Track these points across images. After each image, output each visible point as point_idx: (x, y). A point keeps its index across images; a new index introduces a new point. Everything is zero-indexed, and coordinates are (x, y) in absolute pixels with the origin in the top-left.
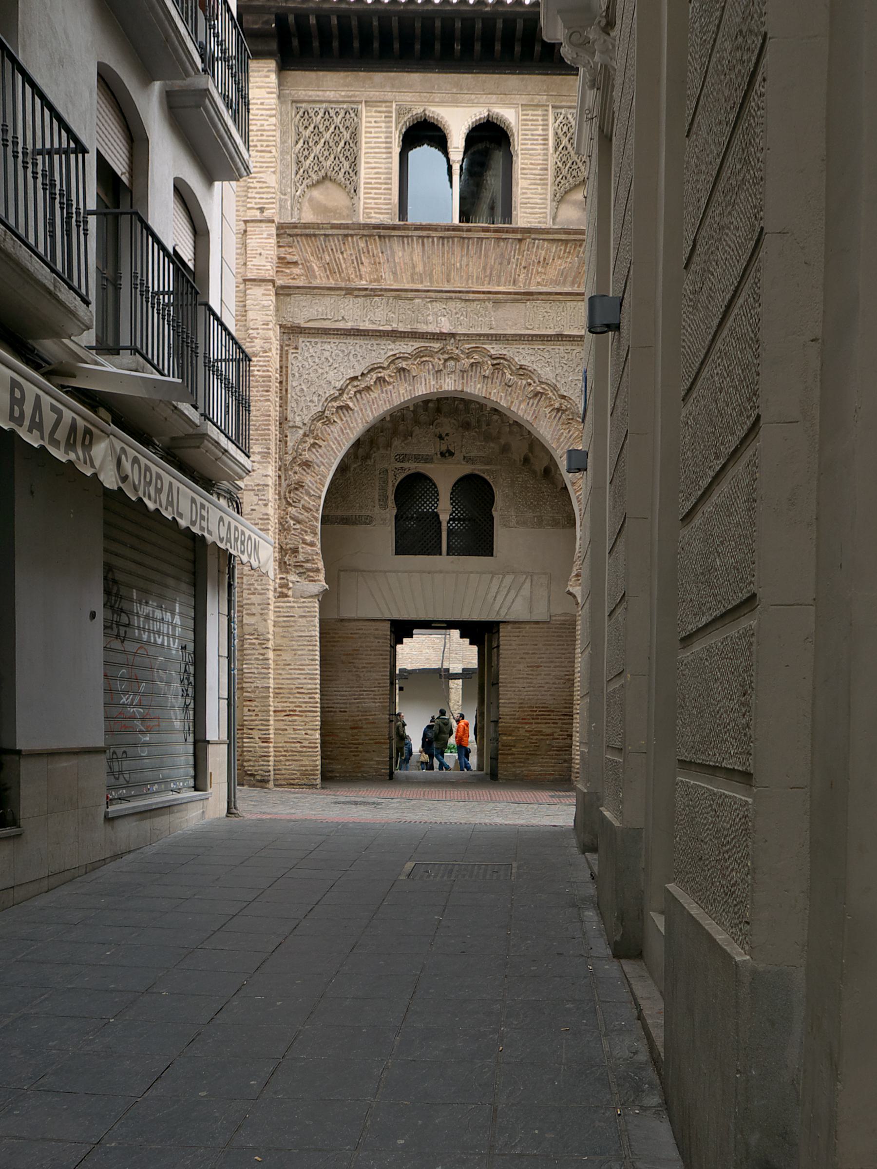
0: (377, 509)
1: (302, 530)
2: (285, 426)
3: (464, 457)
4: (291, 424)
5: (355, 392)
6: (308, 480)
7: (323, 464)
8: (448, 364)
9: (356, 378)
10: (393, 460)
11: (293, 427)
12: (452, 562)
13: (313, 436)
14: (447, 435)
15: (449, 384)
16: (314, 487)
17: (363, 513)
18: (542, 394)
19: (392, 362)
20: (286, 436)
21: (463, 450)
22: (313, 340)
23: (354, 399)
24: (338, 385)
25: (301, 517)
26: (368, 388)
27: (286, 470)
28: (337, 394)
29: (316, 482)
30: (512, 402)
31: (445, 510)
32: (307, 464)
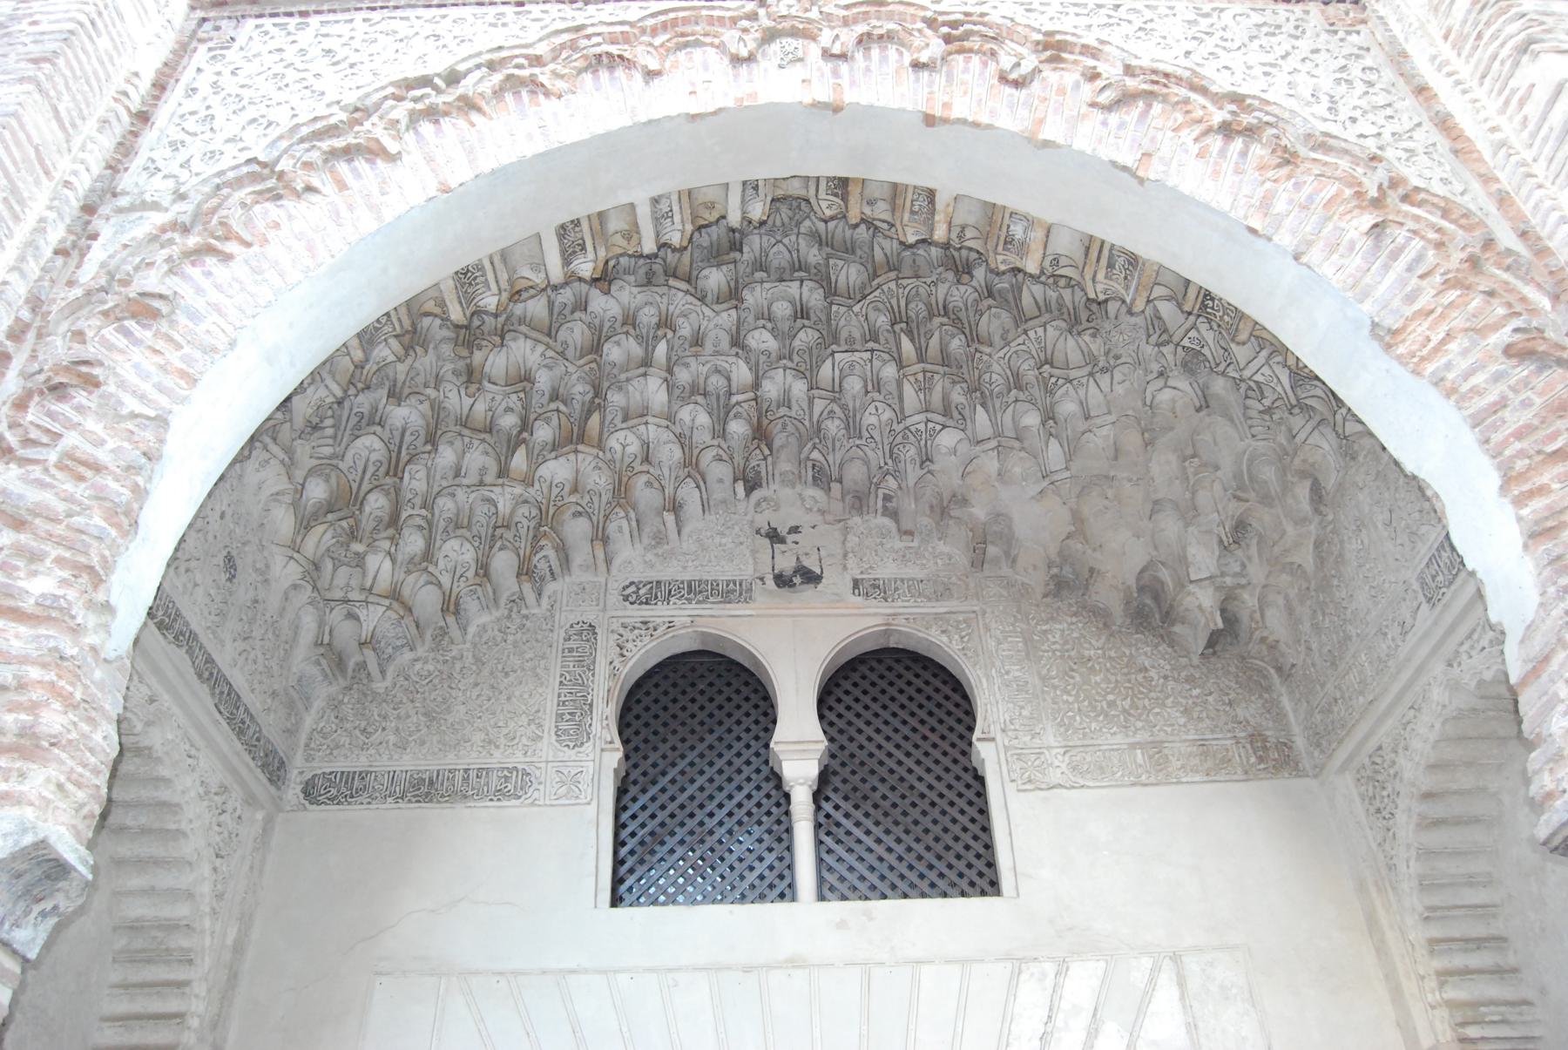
0: (548, 748)
1: (19, 550)
2: (105, 210)
3: (856, 584)
4: (123, 202)
5: (414, 118)
6: (131, 363)
7: (219, 311)
8: (775, 47)
9: (425, 81)
10: (614, 598)
11: (132, 208)
12: (842, 925)
13: (206, 236)
14: (795, 530)
15: (784, 82)
16: (146, 387)
17: (497, 759)
18: (1151, 94)
19: (573, 45)
20: (94, 237)
21: (851, 562)
22: (293, 22)
23: (409, 137)
24: (351, 98)
25: (34, 496)
26: (468, 105)
27: (40, 336)
28: (344, 116)
29: (163, 368)
30: (1041, 122)
31: (799, 746)
32: (145, 309)
